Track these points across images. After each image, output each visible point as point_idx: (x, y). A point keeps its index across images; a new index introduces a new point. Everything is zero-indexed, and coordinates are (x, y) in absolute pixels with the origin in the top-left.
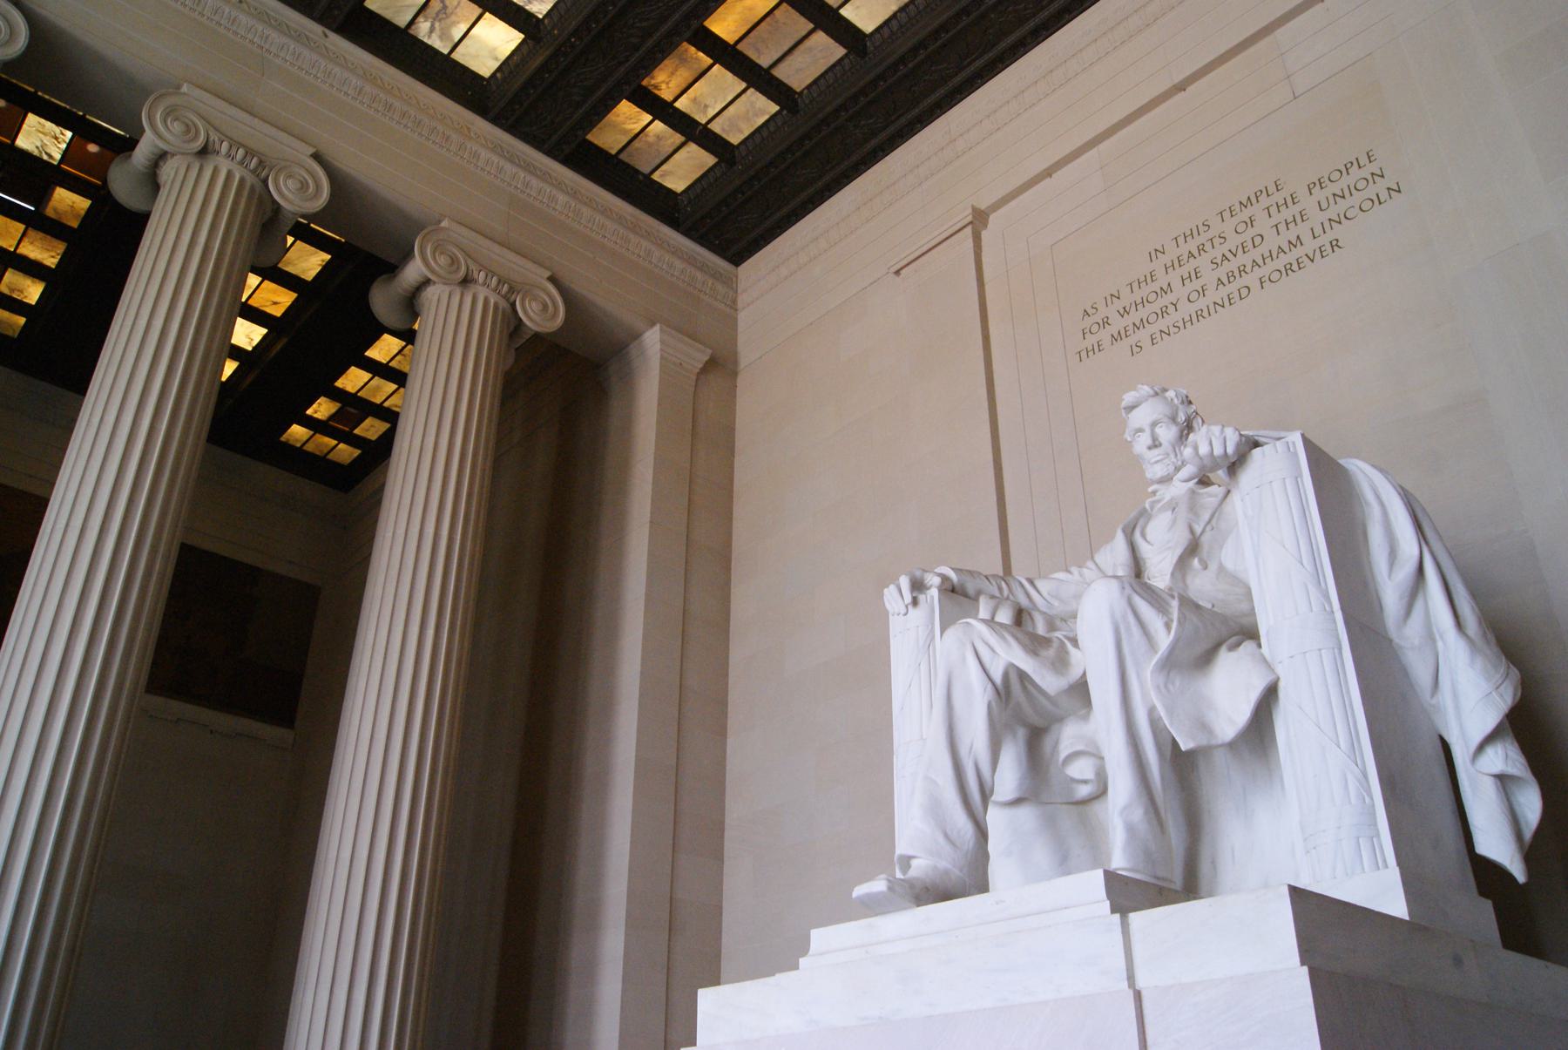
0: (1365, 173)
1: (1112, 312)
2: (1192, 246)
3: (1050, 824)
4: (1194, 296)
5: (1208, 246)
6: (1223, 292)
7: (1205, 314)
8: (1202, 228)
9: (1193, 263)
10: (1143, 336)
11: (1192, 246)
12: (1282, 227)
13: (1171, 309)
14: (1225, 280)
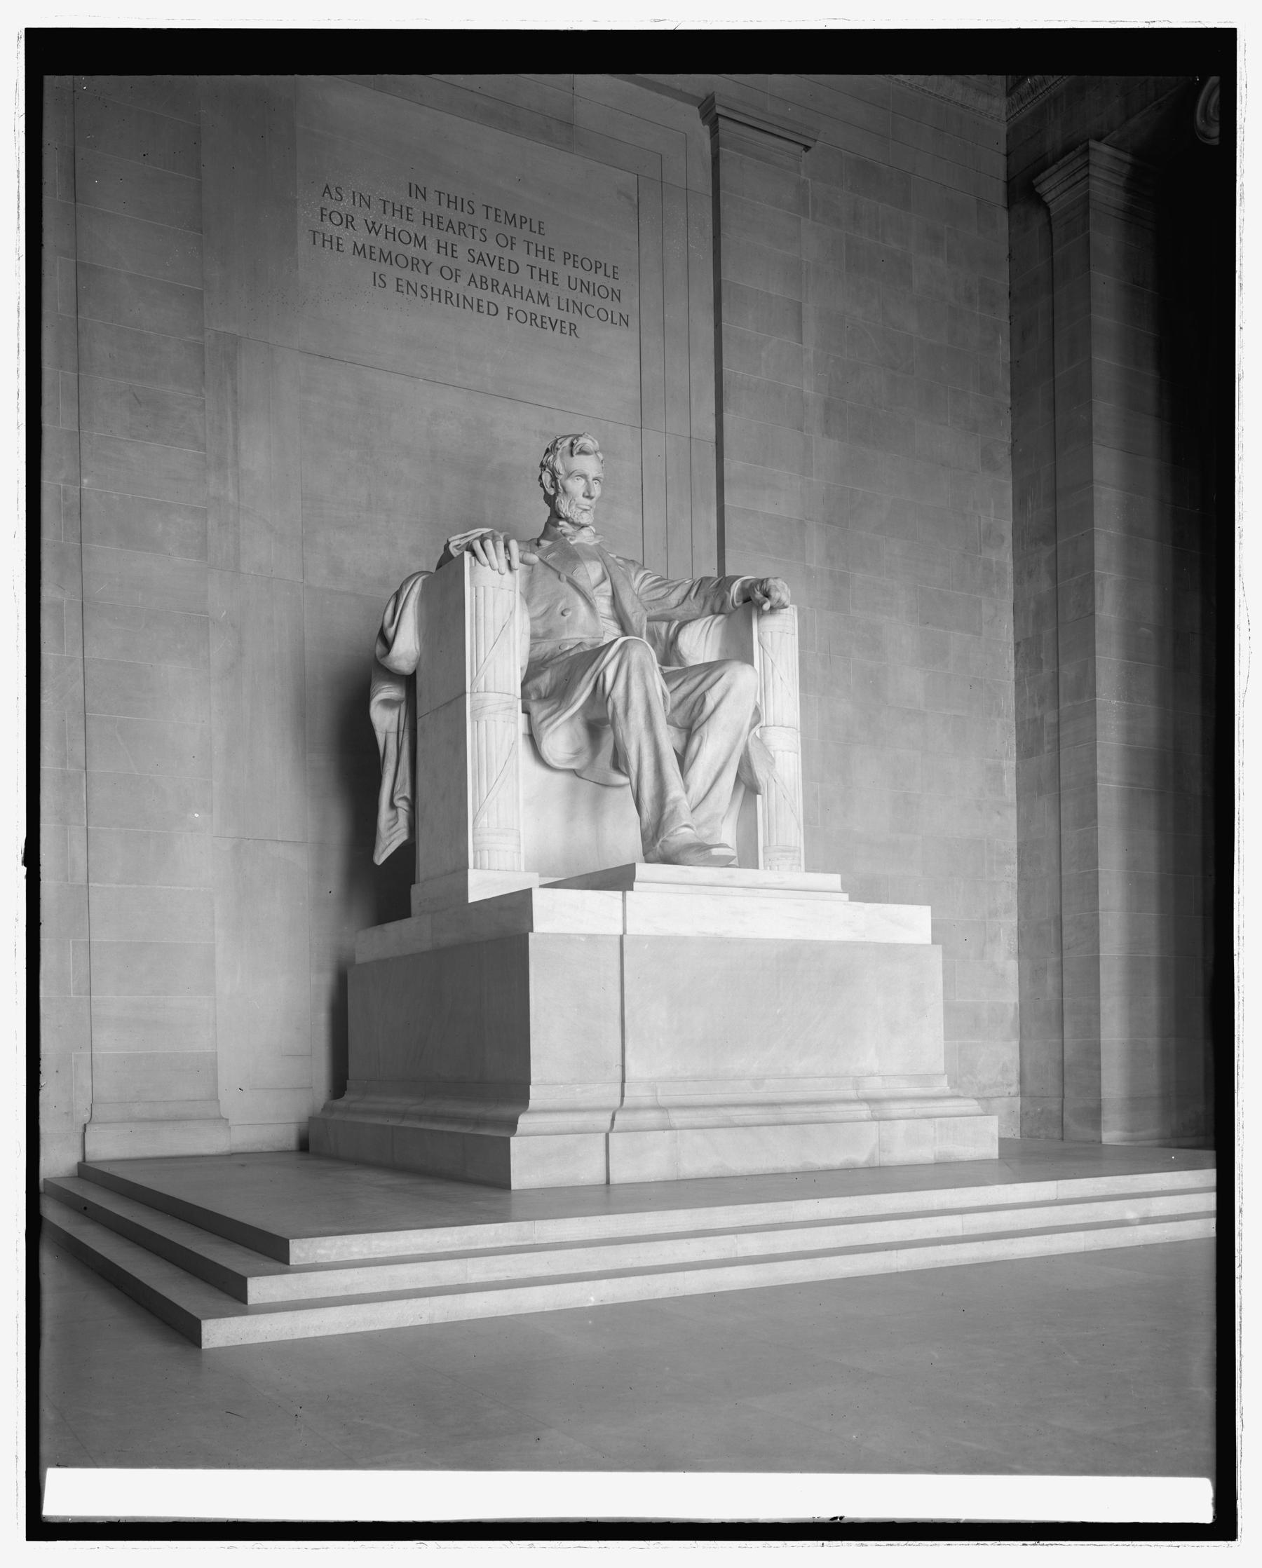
0: (611, 283)
1: (360, 215)
2: (457, 216)
3: (573, 791)
4: (447, 273)
5: (469, 231)
6: (474, 293)
7: (454, 299)
8: (466, 207)
9: (449, 237)
10: (391, 272)
11: (457, 216)
12: (536, 272)
13: (421, 266)
14: (478, 279)
